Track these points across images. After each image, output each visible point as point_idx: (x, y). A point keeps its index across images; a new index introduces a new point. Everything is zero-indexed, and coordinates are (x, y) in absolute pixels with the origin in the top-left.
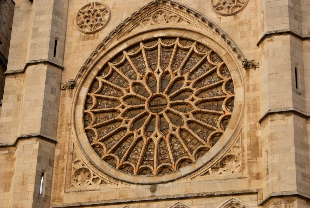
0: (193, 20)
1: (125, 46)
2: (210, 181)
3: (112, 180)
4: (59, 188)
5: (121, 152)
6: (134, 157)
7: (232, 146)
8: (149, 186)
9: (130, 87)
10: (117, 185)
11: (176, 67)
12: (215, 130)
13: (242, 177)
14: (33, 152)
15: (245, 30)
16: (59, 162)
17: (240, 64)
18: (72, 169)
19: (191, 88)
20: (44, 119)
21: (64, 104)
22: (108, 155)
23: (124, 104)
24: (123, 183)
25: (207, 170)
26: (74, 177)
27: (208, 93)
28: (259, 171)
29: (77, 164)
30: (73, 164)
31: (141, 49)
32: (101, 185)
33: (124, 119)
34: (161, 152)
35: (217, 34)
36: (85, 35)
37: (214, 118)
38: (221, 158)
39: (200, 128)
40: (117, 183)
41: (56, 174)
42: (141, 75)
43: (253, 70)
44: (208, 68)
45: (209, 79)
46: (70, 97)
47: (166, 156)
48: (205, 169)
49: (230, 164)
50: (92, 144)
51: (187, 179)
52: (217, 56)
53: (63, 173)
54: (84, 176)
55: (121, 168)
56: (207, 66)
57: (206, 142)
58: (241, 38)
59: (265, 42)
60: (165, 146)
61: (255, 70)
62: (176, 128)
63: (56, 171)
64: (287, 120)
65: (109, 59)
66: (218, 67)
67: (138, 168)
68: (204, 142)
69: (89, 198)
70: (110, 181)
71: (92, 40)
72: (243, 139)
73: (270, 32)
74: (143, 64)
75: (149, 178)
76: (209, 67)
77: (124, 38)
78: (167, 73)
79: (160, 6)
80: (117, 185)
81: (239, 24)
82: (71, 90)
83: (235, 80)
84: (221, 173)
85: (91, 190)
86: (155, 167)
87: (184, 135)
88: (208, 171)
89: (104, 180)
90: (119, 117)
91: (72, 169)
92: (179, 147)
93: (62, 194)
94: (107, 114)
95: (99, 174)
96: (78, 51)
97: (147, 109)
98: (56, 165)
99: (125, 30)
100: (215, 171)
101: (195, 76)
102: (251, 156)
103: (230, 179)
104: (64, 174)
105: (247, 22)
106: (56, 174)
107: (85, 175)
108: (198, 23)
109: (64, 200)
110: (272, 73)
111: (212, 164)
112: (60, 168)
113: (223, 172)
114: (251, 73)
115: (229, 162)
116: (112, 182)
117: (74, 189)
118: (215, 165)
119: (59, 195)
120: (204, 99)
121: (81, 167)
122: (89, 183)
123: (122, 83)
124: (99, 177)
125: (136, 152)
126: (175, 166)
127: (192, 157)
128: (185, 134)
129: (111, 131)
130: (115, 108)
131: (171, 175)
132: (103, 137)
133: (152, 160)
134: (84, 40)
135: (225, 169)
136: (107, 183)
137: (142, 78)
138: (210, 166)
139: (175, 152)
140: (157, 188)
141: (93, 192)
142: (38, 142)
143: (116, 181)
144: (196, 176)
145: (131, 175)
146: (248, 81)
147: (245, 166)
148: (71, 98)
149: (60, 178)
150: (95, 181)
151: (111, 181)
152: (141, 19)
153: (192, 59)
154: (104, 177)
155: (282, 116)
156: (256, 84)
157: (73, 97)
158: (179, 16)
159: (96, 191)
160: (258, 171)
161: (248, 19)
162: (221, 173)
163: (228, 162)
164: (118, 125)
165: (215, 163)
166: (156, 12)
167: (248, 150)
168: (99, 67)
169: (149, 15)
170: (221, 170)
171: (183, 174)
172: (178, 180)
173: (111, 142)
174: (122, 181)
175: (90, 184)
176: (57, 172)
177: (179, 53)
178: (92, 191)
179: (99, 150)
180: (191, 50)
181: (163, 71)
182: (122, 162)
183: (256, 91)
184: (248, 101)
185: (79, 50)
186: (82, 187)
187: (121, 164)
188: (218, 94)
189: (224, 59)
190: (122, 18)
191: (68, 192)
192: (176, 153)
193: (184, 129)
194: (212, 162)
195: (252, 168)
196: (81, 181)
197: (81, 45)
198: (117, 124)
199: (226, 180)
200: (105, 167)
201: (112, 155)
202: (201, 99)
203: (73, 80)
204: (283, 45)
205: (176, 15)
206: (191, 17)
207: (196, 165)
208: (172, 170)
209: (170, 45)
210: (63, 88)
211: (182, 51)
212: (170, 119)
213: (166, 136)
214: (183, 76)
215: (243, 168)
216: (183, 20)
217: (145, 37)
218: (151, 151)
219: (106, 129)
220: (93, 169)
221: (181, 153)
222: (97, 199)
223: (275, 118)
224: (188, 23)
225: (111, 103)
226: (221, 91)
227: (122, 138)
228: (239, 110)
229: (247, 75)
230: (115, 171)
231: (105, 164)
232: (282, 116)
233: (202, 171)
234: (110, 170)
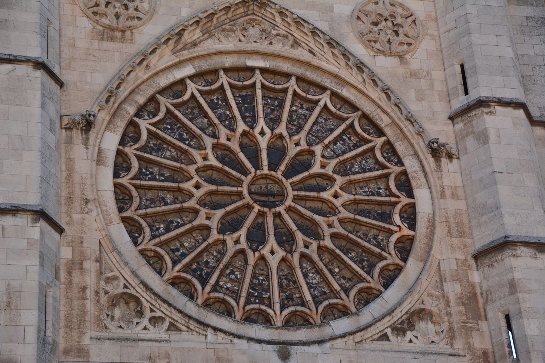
0: (321, 50)
1: (188, 70)
2: (395, 352)
3: (193, 325)
4: (76, 327)
5: (201, 274)
6: (229, 285)
7: (425, 293)
8: (275, 347)
9: (209, 151)
10: (206, 336)
11: (294, 130)
12: (385, 258)
13: (453, 353)
14: (28, 243)
15: (423, 88)
16: (73, 275)
17: (421, 146)
18: (102, 293)
19: (331, 173)
20: (45, 180)
21: (71, 157)
22: (176, 274)
23: (200, 181)
24: (219, 333)
25: (385, 331)
26: (106, 308)
27: (361, 188)
28: (485, 348)
29: (110, 284)
30: (102, 283)
31: (222, 84)
32: (170, 332)
33: (201, 208)
34: (284, 285)
35: (372, 84)
36: (103, 31)
37: (378, 236)
38: (407, 312)
39: (354, 251)
40: (204, 333)
41: (68, 298)
42: (228, 132)
43: (448, 161)
44: (356, 143)
45: (360, 162)
46: (83, 146)
47: (295, 294)
48: (381, 329)
49: (422, 325)
50: (139, 248)
51: (347, 343)
52: (369, 125)
53: (84, 298)
54: (127, 311)
55: (206, 305)
56: (352, 138)
57: (372, 277)
58: (417, 99)
59: (475, 114)
60: (289, 273)
61: (451, 161)
62: (311, 244)
63: (67, 293)
64: (542, 259)
65: (158, 88)
66: (378, 145)
67: (244, 308)
68: (369, 278)
69: (149, 356)
70: (188, 328)
71: (121, 44)
72: (444, 283)
73: (487, 98)
74: (228, 112)
75: (269, 330)
76: (357, 141)
77: (186, 54)
78: (281, 137)
79: (253, 10)
80: (206, 336)
81: (411, 74)
82: (85, 133)
83: (413, 173)
84: (411, 341)
85: (150, 340)
86: (278, 312)
87: (326, 258)
88: (387, 332)
89: (176, 324)
90: (192, 203)
91: (102, 293)
92: (317, 279)
93: (86, 341)
94: (162, 194)
95: (162, 309)
96: (93, 58)
97: (248, 199)
98: (66, 278)
99: (187, 37)
100: (398, 335)
101: (332, 153)
102: (467, 317)
103: (432, 353)
104: (87, 299)
105: (424, 73)
106: (68, 298)
107: (129, 308)
108: (332, 56)
109: (91, 354)
110: (500, 171)
111: (392, 322)
112: (75, 286)
113: (414, 339)
114: (444, 165)
115: (421, 322)
116: (192, 330)
117: (110, 334)
118: (396, 323)
119: (78, 342)
120: (358, 197)
121: (121, 290)
122: (142, 326)
123: (187, 139)
124: (163, 316)
125: (233, 276)
126: (319, 316)
127: (350, 301)
128: (326, 256)
129: (177, 227)
130: (182, 185)
131: (314, 330)
132: (163, 238)
133: (267, 296)
134: (102, 39)
135: (414, 333)
136: (180, 330)
137: (230, 137)
138: (389, 324)
139: (312, 288)
140: (291, 353)
141: (157, 344)
142: (38, 225)
143: (202, 327)
144: (363, 340)
145: (231, 320)
146: (441, 178)
147: (457, 334)
148: (88, 148)
149: (77, 307)
150: (155, 323)
151: (192, 327)
152: (217, 25)
153: (323, 121)
154: (177, 316)
155: (531, 252)
156: (455, 187)
157: (91, 148)
158: (293, 38)
159: (163, 344)
160: (483, 346)
161: (425, 68)
162: (411, 341)
163: (419, 323)
164: (188, 219)
165: (398, 320)
166: (246, 20)
167: (458, 304)
168: (141, 100)
169: (233, 23)
170: (409, 335)
171: (338, 332)
172: (331, 343)
173: (178, 250)
174: (216, 329)
175: (145, 328)
176: (69, 294)
177: (297, 104)
178: (154, 343)
179: (154, 263)
180: (322, 103)
181: (272, 133)
182: (209, 293)
183: (458, 199)
184: (447, 216)
185: (94, 56)
186: (127, 333)
187: (206, 296)
188: (380, 193)
189: (388, 131)
190: (181, 15)
191: (99, 339)
192: (314, 291)
193: (326, 247)
194: (391, 317)
195: (471, 339)
196: (122, 319)
197: (98, 48)
198: (187, 217)
199: (425, 355)
200: (174, 297)
201: (184, 275)
202: (352, 197)
203: (93, 113)
204: (514, 126)
205: (286, 33)
206: (317, 43)
207: (360, 318)
208: (311, 321)
209: (280, 87)
210: (68, 126)
211: (302, 102)
212: (276, 227)
213: (292, 255)
214: (313, 148)
215: (452, 338)
216: (300, 45)
217: (229, 61)
218: (263, 280)
219: (163, 224)
220: (149, 299)
221: (323, 291)
222: (167, 360)
223: (519, 252)
224: (309, 54)
225: (169, 174)
226: (386, 189)
227: (203, 246)
228: (428, 229)
229: (436, 168)
230: (197, 307)
231: (174, 292)
232: (531, 252)
233: (374, 331)
234: (185, 305)
